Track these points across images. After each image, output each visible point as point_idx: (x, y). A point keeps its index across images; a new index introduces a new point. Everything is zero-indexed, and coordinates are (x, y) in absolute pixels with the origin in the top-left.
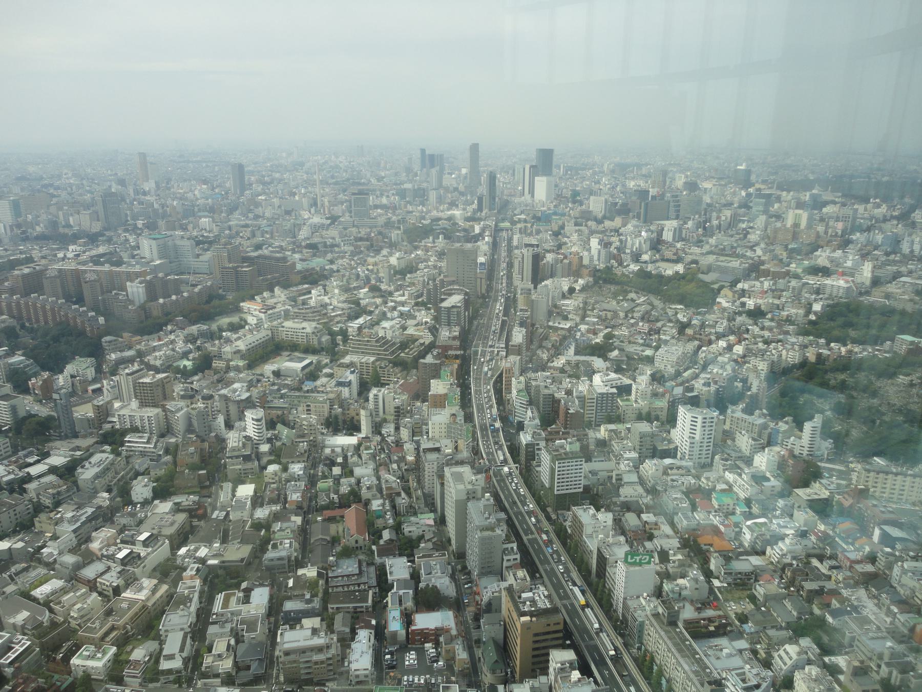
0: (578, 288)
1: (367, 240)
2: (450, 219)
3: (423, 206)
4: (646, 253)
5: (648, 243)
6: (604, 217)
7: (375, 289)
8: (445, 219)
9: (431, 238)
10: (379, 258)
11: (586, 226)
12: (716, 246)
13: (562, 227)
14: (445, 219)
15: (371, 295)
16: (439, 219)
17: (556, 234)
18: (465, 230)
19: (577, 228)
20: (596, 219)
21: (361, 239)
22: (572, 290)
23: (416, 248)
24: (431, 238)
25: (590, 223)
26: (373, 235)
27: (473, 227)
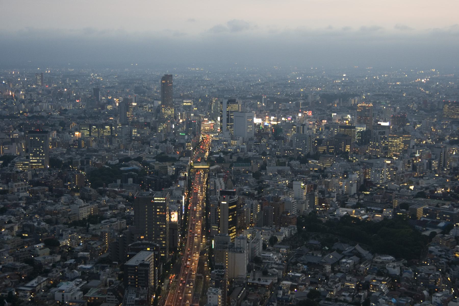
0: (280, 239)
1: (45, 185)
2: (139, 159)
3: (111, 144)
4: (353, 196)
5: (355, 185)
6: (309, 156)
7: (52, 244)
8: (135, 160)
9: (119, 181)
10: (58, 207)
11: (289, 165)
12: (427, 188)
13: (263, 167)
14: (135, 160)
15: (48, 250)
16: (128, 159)
17: (257, 175)
18: (157, 173)
19: (280, 168)
20: (299, 158)
21: (38, 184)
22: (273, 241)
23: (102, 193)
24: (119, 181)
25: (293, 162)
26: (52, 178)
27: (166, 168)
